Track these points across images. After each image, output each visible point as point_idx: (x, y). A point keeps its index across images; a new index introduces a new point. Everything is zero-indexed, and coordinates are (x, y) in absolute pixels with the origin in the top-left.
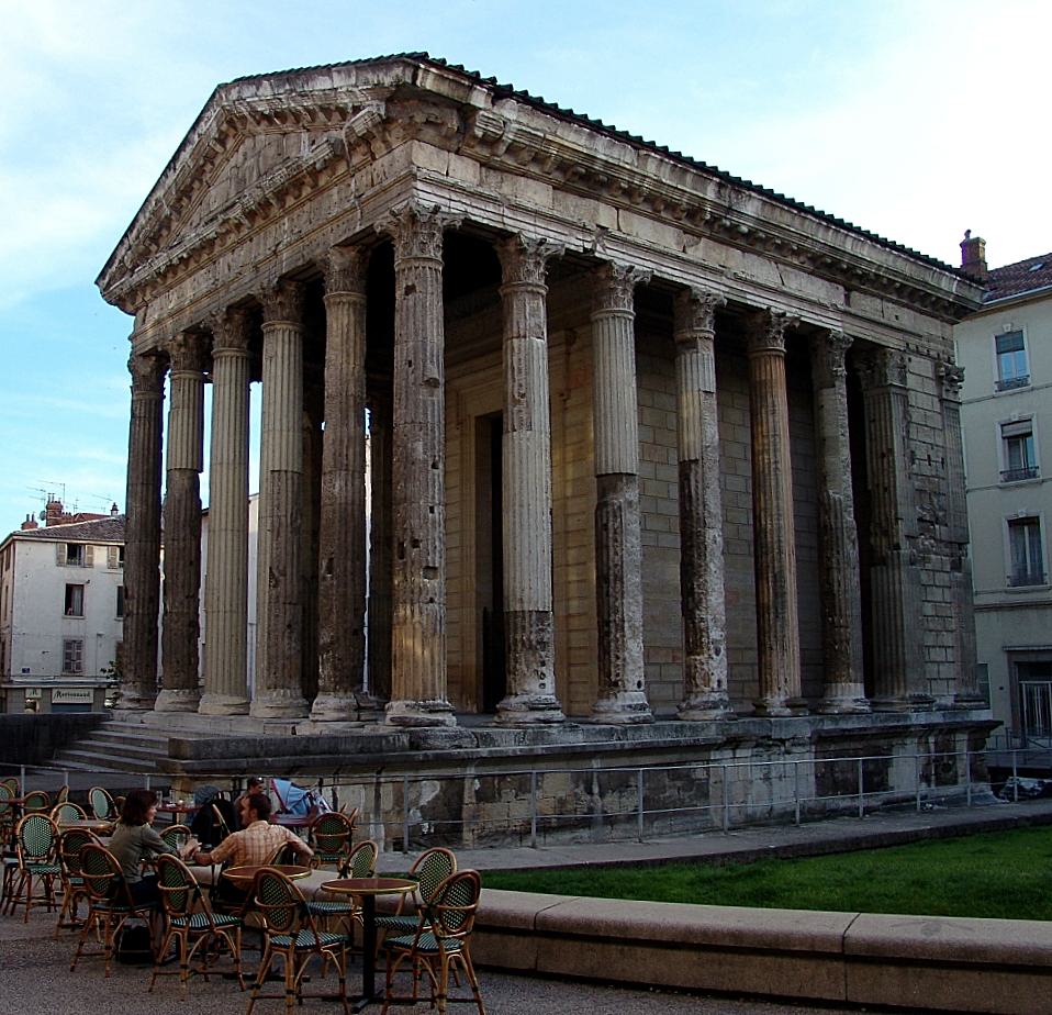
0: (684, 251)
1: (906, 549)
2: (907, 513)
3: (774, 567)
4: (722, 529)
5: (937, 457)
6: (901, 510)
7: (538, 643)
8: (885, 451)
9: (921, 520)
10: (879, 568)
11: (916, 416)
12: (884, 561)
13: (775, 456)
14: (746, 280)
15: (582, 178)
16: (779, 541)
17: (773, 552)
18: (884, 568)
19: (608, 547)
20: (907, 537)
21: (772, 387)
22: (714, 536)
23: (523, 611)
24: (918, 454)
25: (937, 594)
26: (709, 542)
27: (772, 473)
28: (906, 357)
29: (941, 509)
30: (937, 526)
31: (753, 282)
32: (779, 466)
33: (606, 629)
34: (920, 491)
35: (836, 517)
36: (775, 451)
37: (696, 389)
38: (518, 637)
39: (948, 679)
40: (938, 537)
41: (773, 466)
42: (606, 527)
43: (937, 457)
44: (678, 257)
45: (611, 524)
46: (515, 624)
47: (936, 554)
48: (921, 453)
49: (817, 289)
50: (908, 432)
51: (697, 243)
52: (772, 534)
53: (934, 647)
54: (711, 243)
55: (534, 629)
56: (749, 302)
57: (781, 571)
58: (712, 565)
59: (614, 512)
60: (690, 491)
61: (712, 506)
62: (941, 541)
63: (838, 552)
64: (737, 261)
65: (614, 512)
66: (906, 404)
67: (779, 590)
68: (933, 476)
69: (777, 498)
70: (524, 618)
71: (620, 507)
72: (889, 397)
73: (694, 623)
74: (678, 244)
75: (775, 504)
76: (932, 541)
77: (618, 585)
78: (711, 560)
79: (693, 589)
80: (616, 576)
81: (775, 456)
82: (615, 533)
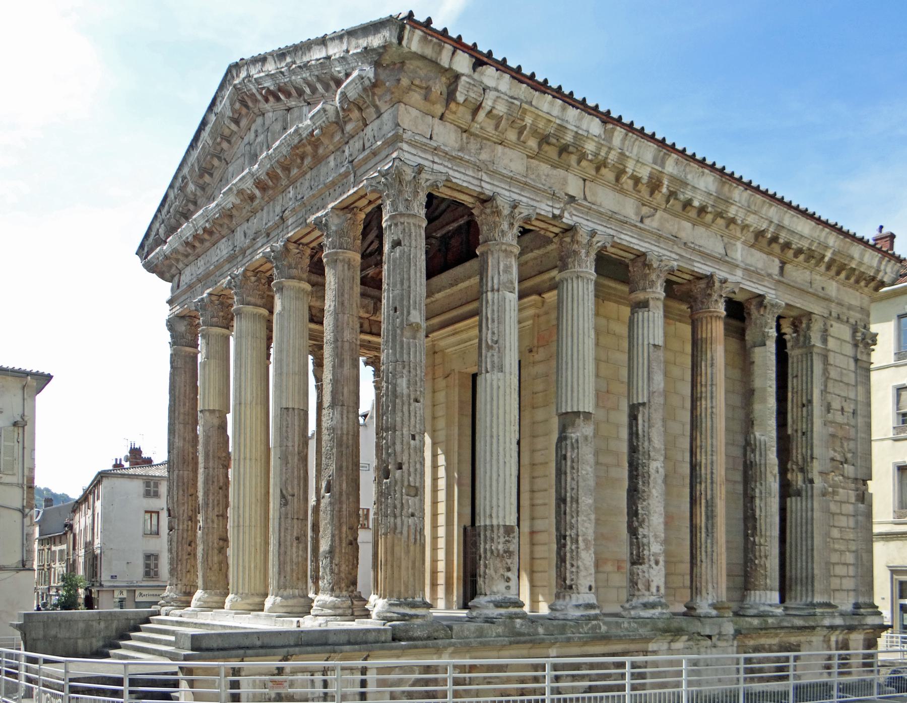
0: (642, 221)
1: (818, 483)
2: (822, 453)
3: (706, 495)
4: (663, 462)
5: (849, 407)
6: (817, 452)
7: (505, 552)
8: (804, 402)
9: (833, 459)
10: (794, 499)
12: (798, 494)
13: (712, 402)
14: (694, 249)
16: (712, 473)
17: (706, 482)
18: (799, 498)
19: (566, 473)
20: (821, 473)
21: (711, 344)
22: (656, 466)
23: (492, 526)
25: (843, 521)
26: (652, 471)
27: (709, 416)
29: (850, 451)
30: (846, 466)
31: (700, 251)
32: (714, 410)
33: (563, 541)
34: (833, 436)
35: (761, 455)
36: (712, 398)
37: (646, 343)
38: (488, 547)
40: (846, 474)
41: (709, 411)
42: (565, 458)
43: (849, 407)
44: (636, 226)
45: (569, 454)
46: (485, 536)
47: (844, 488)
50: (826, 386)
51: (653, 215)
52: (706, 467)
54: (666, 215)
55: (502, 540)
56: (696, 269)
57: (712, 498)
58: (654, 491)
59: (572, 444)
60: (637, 430)
61: (656, 442)
62: (848, 478)
63: (761, 484)
64: (686, 230)
65: (572, 444)
66: (825, 358)
67: (709, 514)
69: (712, 437)
70: (492, 531)
71: (577, 441)
72: (812, 357)
73: (637, 538)
74: (637, 214)
75: (709, 442)
77: (574, 505)
78: (654, 487)
79: (637, 510)
80: (572, 497)
81: (712, 402)
82: (573, 461)
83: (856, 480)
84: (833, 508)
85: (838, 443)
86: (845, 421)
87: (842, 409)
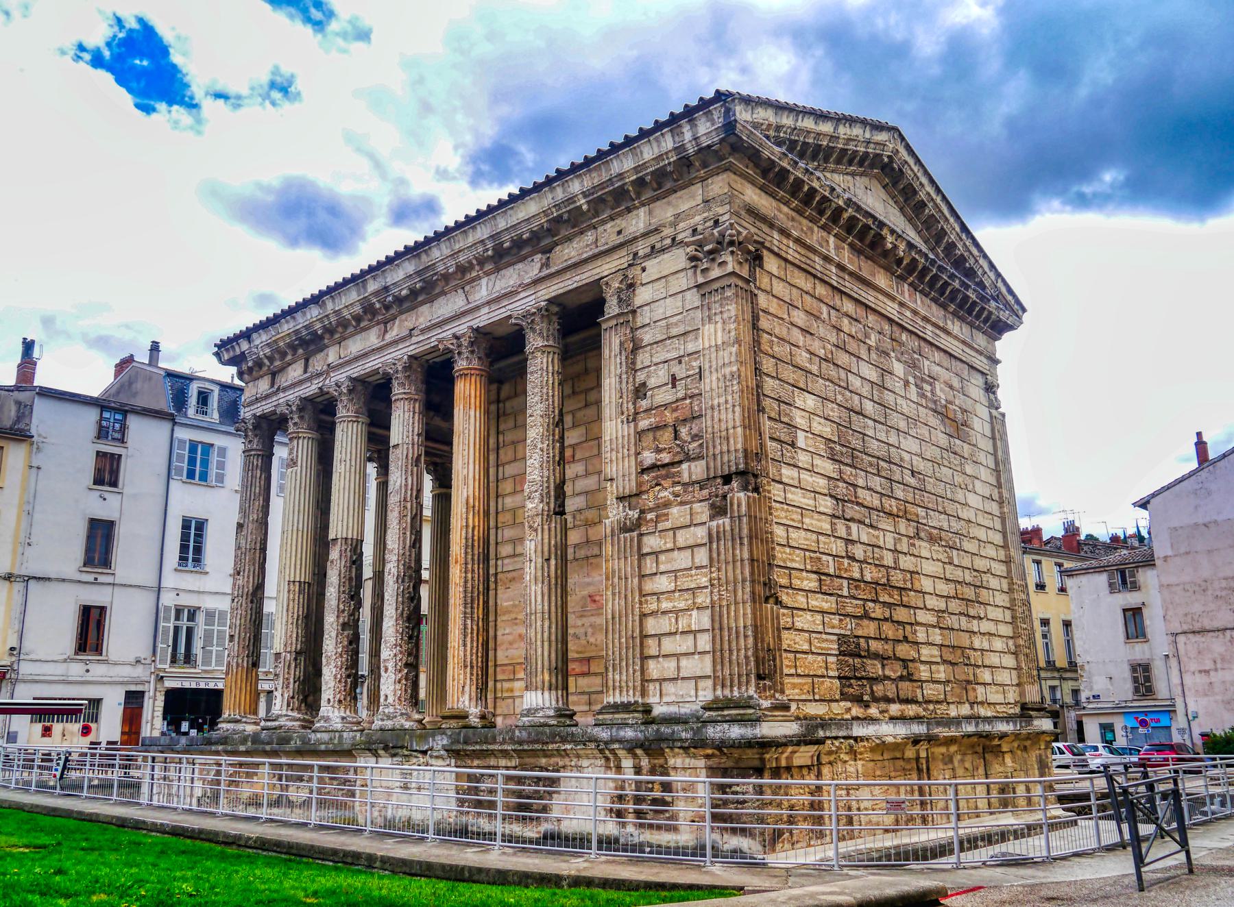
11: (647, 337)
15: (309, 344)
20: (620, 499)
24: (652, 382)
28: (631, 273)
29: (695, 437)
39: (697, 678)
47: (682, 503)
48: (658, 377)
49: (510, 277)
53: (671, 634)
54: (404, 316)
62: (694, 483)
64: (425, 315)
68: (685, 399)
76: (678, 488)
83: (702, 484)
84: (651, 543)
85: (668, 435)
86: (681, 395)
87: (674, 380)
